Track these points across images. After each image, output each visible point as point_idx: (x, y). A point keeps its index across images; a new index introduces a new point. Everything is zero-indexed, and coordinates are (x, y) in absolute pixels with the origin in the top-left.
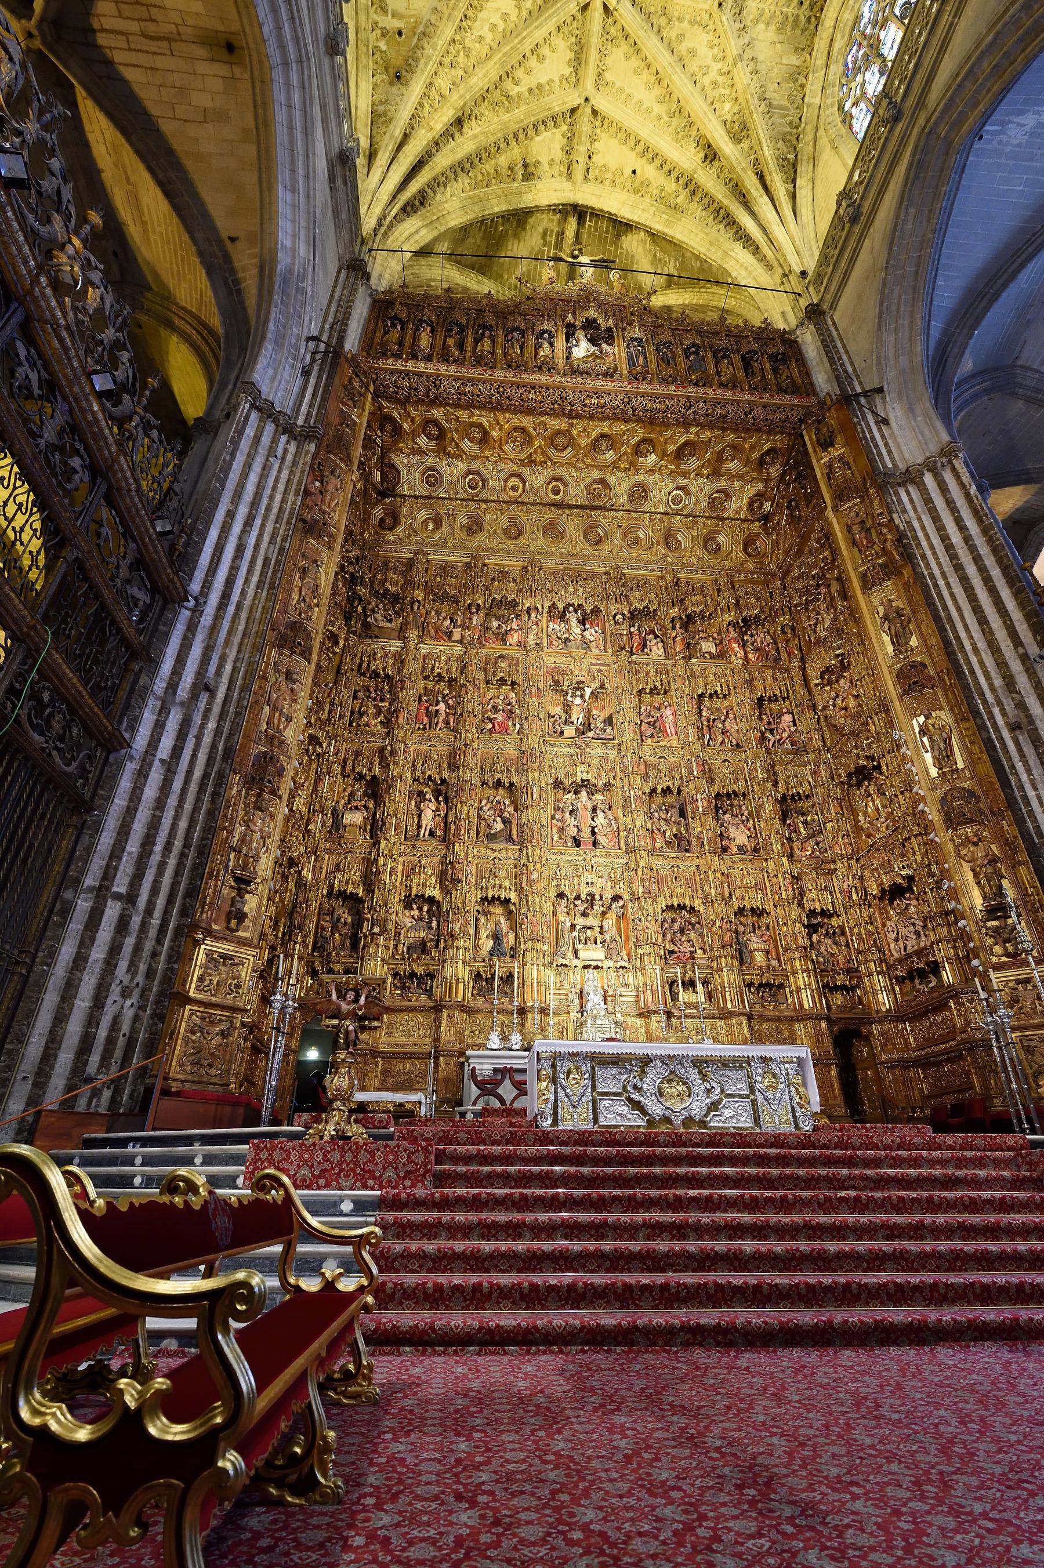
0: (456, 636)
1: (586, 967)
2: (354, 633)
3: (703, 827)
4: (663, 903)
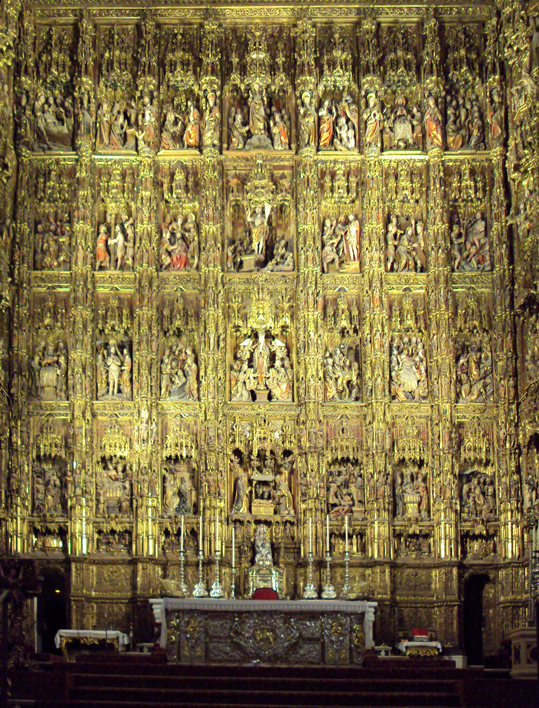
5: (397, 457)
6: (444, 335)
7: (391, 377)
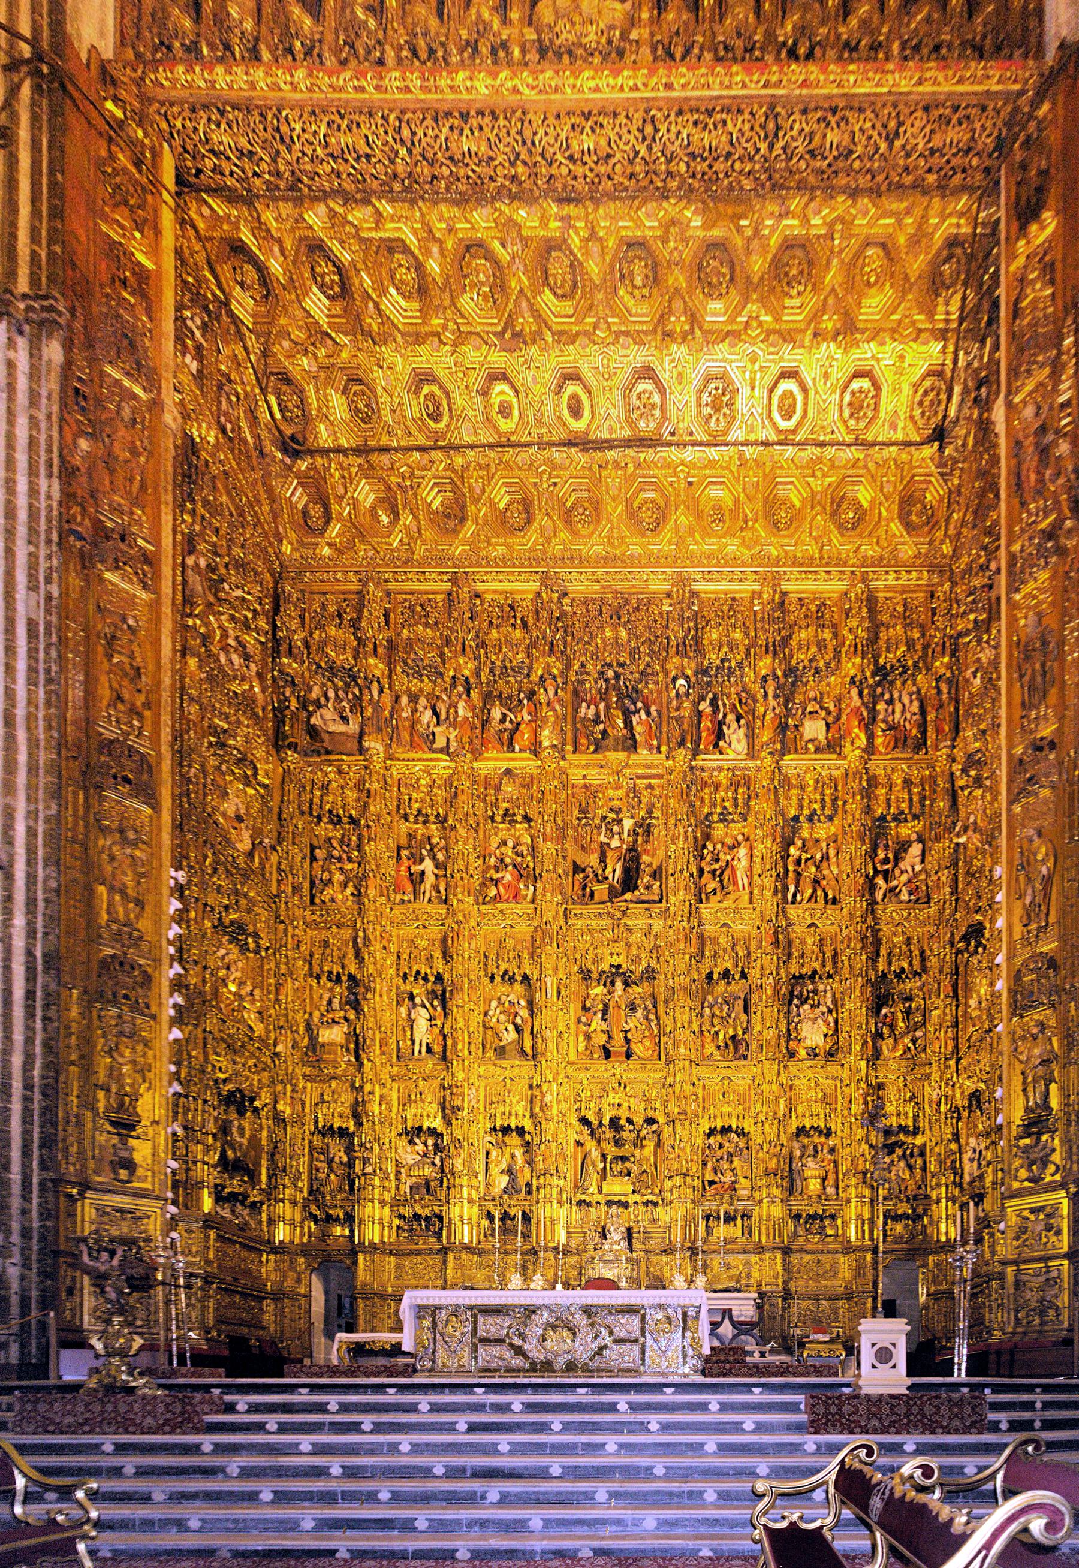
0: (440, 743)
1: (609, 1203)
2: (293, 747)
3: (765, 1024)
4: (705, 1126)
5: (794, 1124)
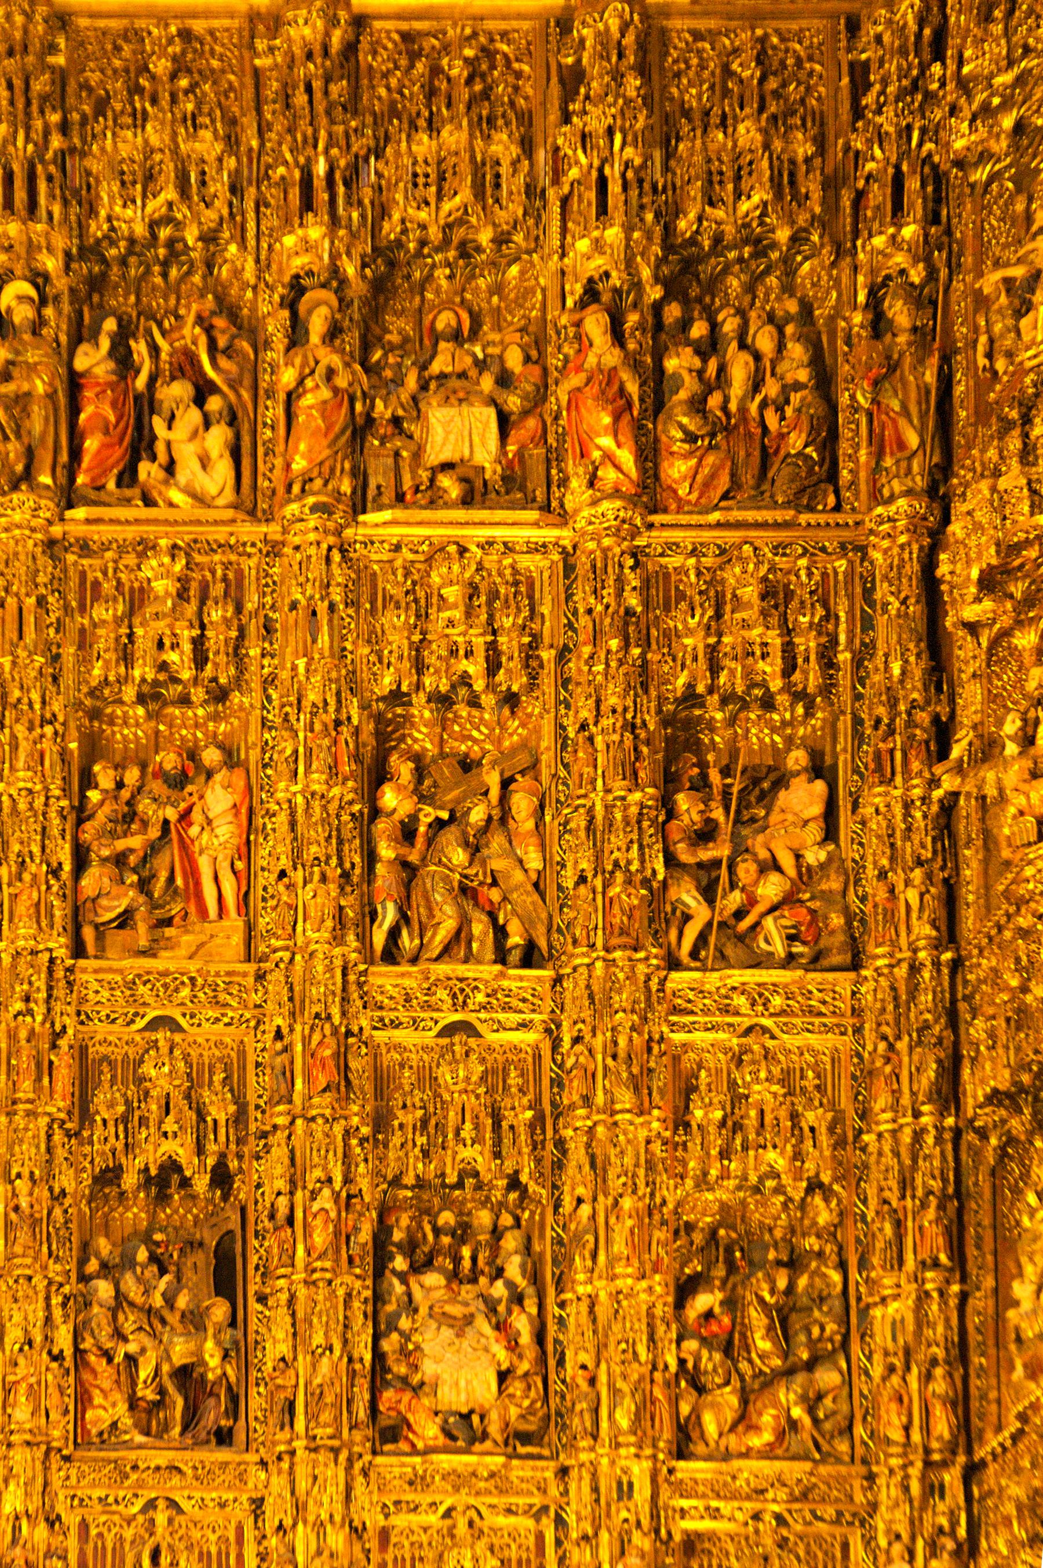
6: (627, 1203)
7: (378, 1356)
